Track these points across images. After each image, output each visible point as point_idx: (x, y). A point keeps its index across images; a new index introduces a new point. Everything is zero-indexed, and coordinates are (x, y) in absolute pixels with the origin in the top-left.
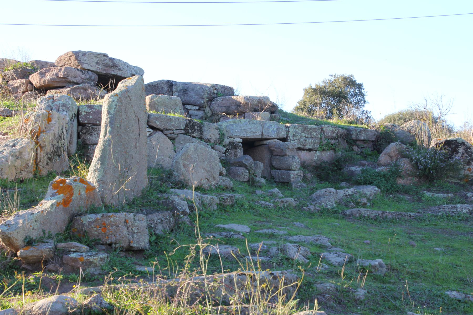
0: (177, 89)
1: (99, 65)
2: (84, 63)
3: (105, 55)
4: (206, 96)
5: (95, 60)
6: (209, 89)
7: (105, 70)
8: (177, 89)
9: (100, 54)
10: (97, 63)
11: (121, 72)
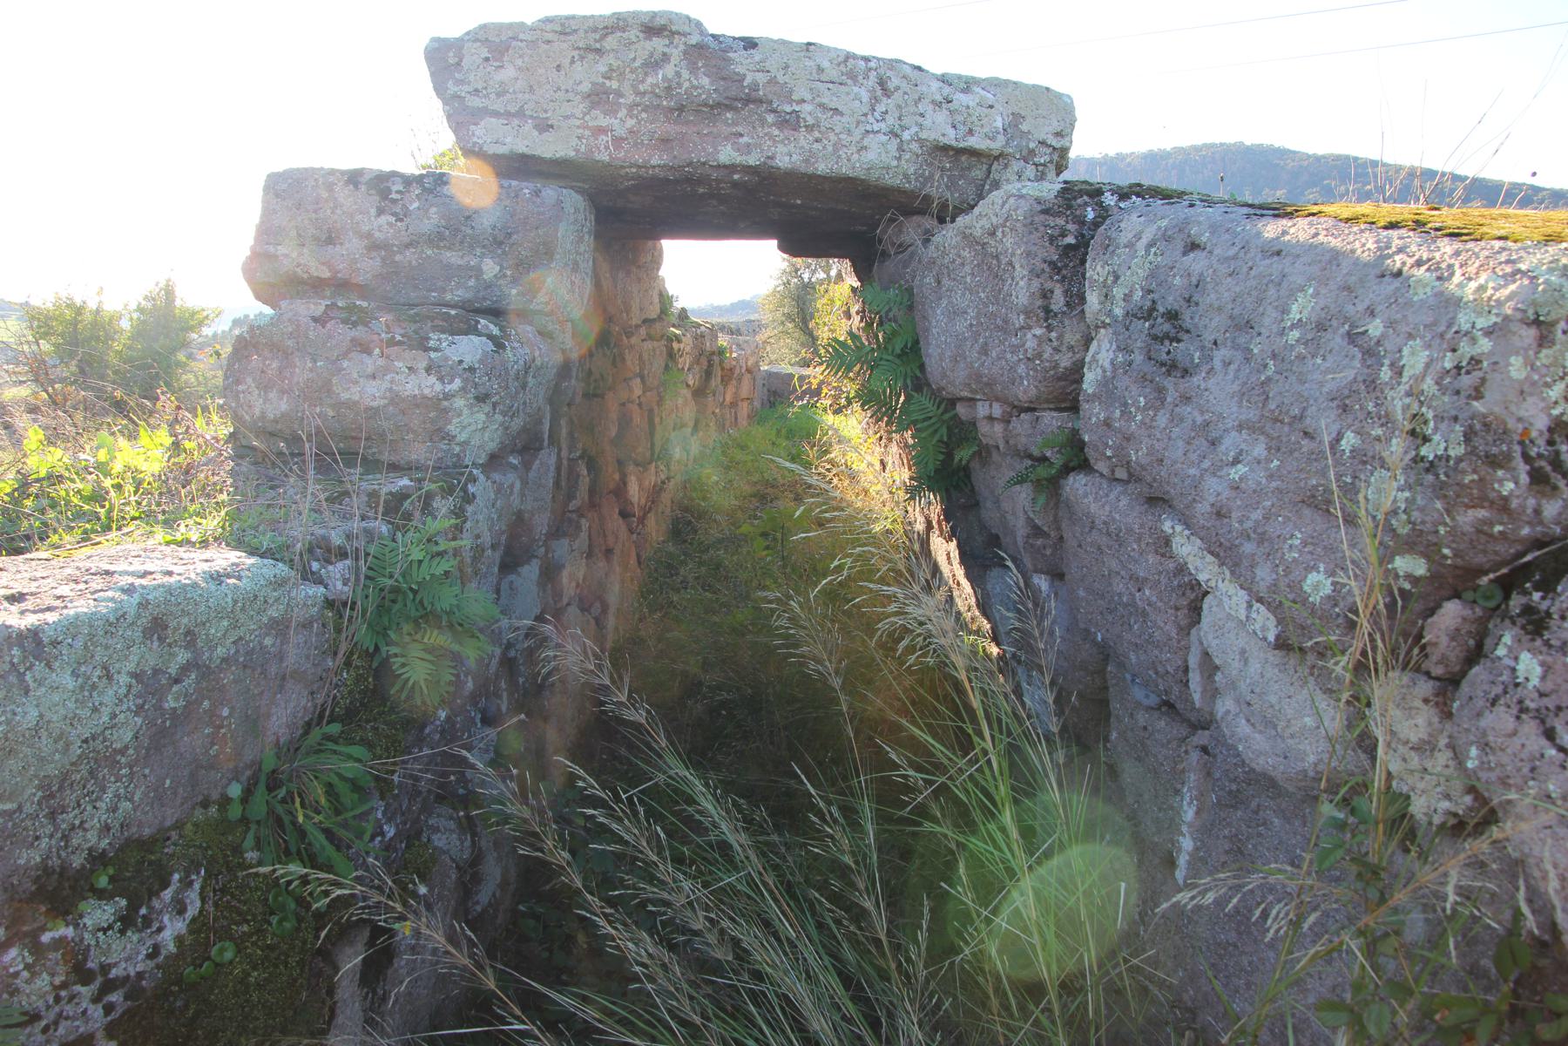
1: (612, 112)
2: (486, 112)
3: (655, 27)
4: (1386, 491)
5: (586, 75)
6: (1468, 378)
7: (665, 141)
9: (616, 25)
10: (599, 98)
11: (804, 139)
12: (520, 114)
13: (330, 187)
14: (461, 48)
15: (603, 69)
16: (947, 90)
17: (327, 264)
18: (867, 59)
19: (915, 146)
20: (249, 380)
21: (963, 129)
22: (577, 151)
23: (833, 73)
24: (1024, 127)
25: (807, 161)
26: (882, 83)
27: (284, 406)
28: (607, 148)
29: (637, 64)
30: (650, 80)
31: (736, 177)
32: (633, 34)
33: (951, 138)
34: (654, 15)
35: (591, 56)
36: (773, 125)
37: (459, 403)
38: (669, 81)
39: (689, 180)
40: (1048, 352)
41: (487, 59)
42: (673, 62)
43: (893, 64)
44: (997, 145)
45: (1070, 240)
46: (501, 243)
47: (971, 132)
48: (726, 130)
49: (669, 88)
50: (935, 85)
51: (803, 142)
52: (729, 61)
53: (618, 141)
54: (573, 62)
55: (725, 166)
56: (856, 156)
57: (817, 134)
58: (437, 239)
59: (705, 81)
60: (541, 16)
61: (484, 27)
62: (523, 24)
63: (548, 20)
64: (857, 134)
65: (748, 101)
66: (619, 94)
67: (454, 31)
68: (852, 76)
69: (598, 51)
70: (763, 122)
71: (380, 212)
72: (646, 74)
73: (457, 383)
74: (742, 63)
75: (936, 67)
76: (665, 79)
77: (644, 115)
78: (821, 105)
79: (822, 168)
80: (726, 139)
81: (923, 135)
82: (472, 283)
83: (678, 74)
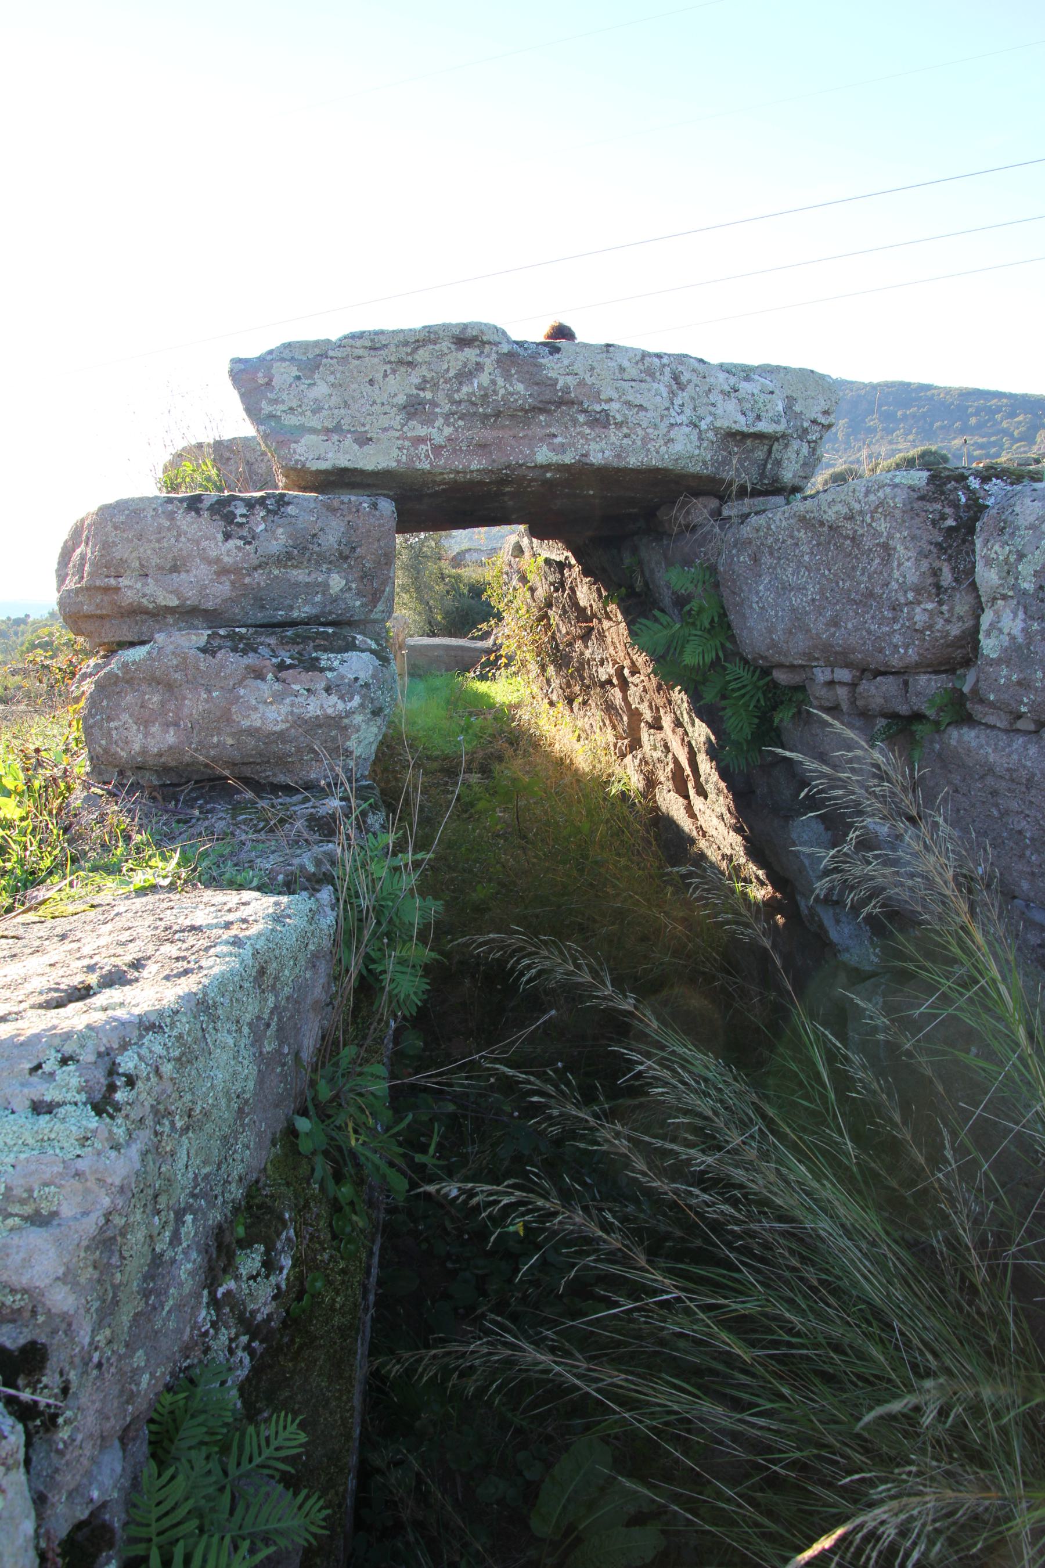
0: (1009, 570)
1: (429, 422)
2: (304, 430)
3: (466, 338)
5: (399, 387)
7: (483, 446)
8: (1009, 570)
9: (428, 337)
10: (414, 409)
11: (614, 435)
12: (337, 429)
13: (171, 516)
14: (270, 368)
15: (416, 381)
16: (733, 380)
17: (176, 593)
18: (659, 356)
19: (711, 435)
20: (125, 717)
21: (751, 416)
22: (398, 461)
23: (633, 372)
24: (797, 408)
25: (618, 456)
26: (676, 378)
27: (172, 738)
28: (427, 456)
29: (451, 374)
30: (465, 389)
31: (549, 475)
32: (445, 345)
33: (742, 424)
34: (465, 327)
35: (403, 369)
36: (585, 424)
37: (358, 719)
38: (486, 389)
39: (503, 481)
40: (940, 623)
41: (298, 378)
42: (487, 370)
43: (682, 358)
44: (781, 428)
45: (950, 522)
46: (347, 558)
47: (759, 418)
48: (540, 432)
49: (486, 395)
50: (722, 376)
51: (613, 439)
52: (540, 366)
53: (437, 449)
54: (385, 376)
55: (542, 467)
56: (664, 449)
57: (625, 430)
58: (285, 559)
59: (520, 387)
60: (346, 331)
61: (288, 346)
62: (328, 342)
63: (353, 336)
64: (663, 427)
65: (561, 403)
66: (434, 404)
67: (253, 351)
68: (650, 373)
69: (410, 364)
70: (575, 421)
71: (227, 536)
72: (461, 383)
73: (357, 700)
74: (552, 367)
75: (714, 358)
76: (480, 386)
77: (461, 423)
78: (628, 403)
79: (632, 461)
80: (541, 440)
81: (718, 424)
82: (318, 598)
83: (494, 382)
